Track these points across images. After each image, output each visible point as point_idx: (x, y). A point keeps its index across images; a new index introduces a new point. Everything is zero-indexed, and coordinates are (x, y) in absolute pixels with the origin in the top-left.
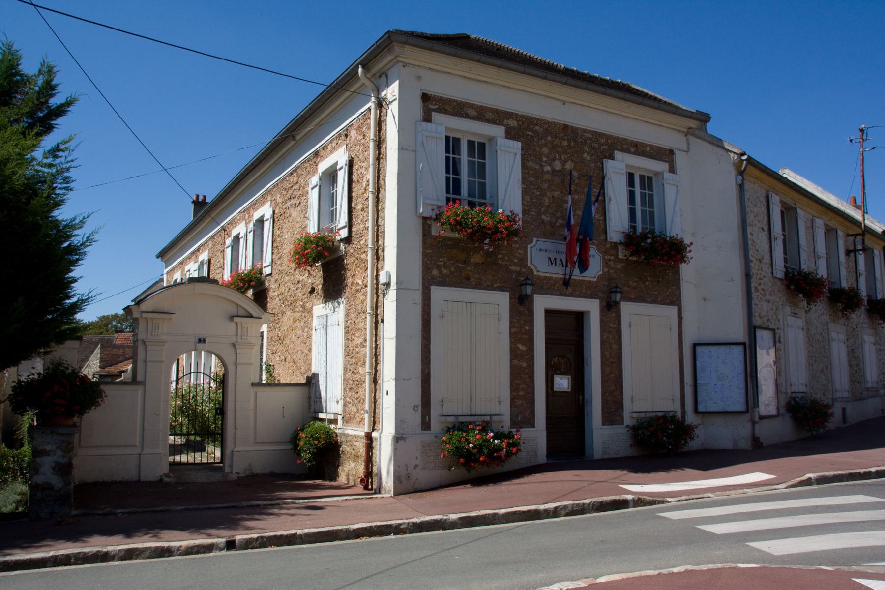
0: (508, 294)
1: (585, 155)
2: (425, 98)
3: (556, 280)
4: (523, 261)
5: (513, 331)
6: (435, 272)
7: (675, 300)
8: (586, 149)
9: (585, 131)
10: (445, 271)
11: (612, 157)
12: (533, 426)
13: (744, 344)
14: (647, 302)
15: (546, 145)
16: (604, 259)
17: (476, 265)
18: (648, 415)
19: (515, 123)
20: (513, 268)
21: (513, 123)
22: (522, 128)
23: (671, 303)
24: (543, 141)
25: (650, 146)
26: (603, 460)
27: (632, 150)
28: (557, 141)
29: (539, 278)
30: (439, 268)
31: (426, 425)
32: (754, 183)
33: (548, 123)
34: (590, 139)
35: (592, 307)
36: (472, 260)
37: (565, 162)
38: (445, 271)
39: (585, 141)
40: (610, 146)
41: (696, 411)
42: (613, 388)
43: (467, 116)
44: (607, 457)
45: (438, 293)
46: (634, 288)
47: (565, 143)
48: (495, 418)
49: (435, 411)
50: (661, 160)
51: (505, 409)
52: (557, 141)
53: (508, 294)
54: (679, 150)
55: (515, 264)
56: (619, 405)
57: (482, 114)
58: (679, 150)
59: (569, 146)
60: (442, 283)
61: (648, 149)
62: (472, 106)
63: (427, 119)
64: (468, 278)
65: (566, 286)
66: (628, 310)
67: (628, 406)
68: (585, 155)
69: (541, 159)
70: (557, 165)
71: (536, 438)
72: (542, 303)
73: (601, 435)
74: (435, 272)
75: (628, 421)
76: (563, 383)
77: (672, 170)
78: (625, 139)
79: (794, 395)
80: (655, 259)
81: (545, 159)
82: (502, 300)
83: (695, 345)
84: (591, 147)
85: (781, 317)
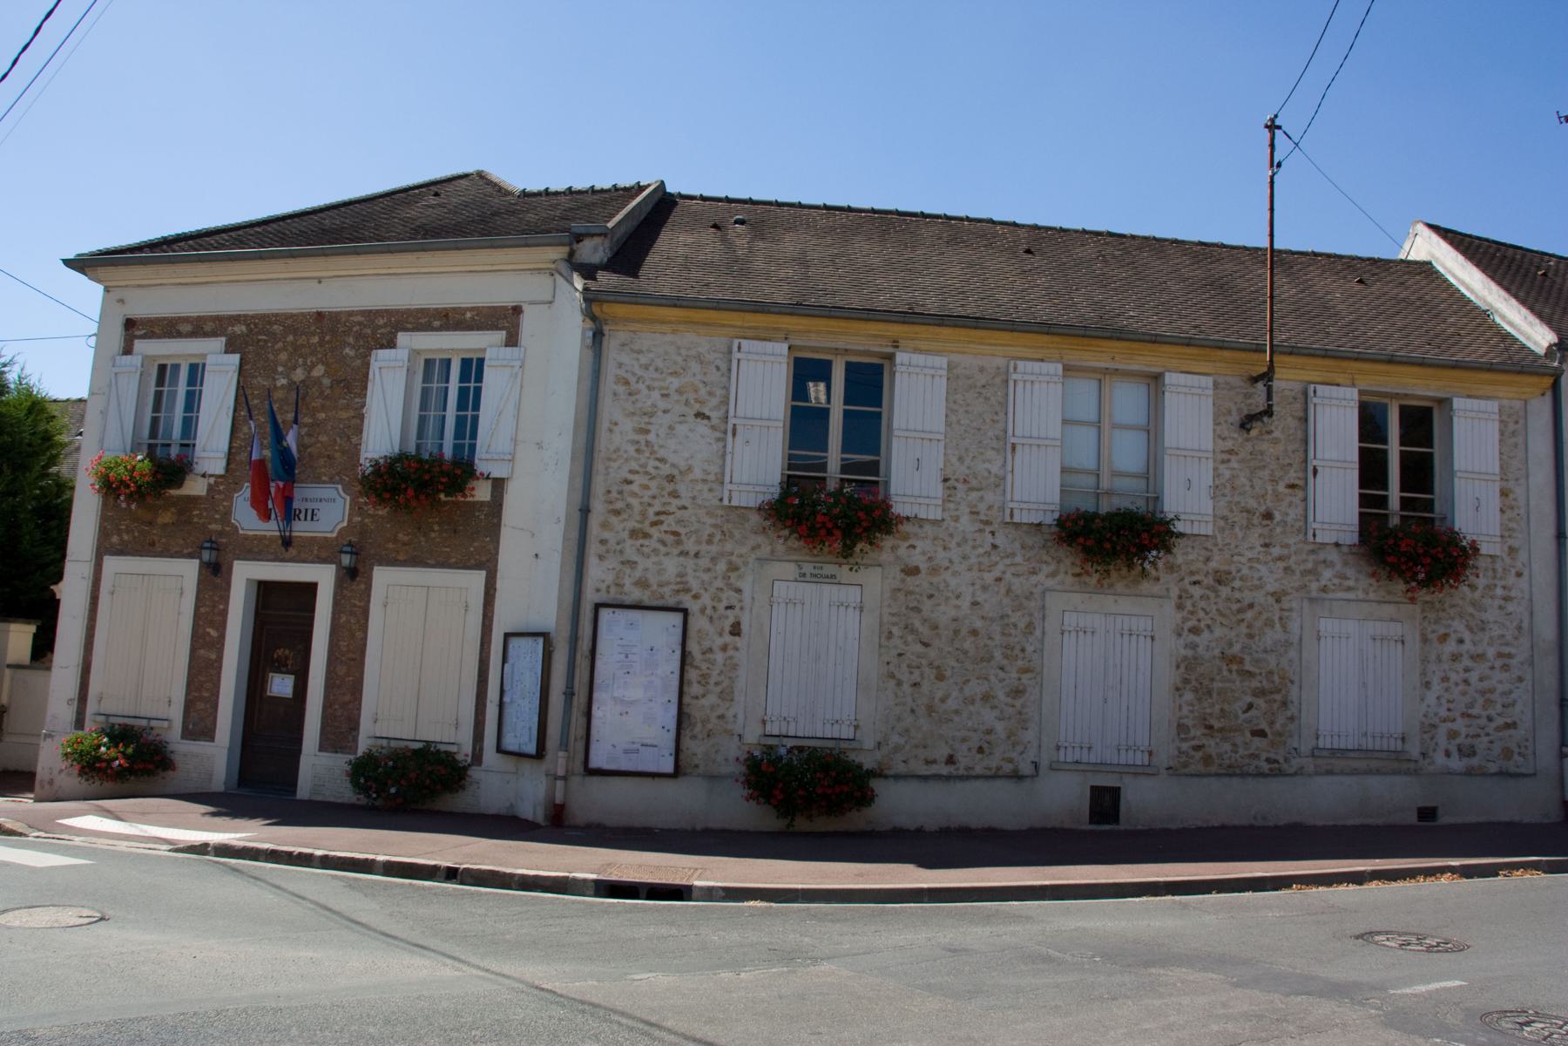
0: (236, 563)
1: (347, 350)
2: (130, 324)
3: (271, 539)
4: (227, 513)
5: (202, 610)
6: (115, 539)
7: (488, 563)
8: (351, 340)
9: (351, 314)
10: (126, 537)
11: (391, 344)
12: (212, 739)
13: (545, 635)
14: (426, 565)
15: (284, 349)
16: (354, 502)
17: (165, 525)
18: (393, 744)
19: (244, 328)
20: (213, 527)
21: (240, 329)
22: (250, 337)
23: (478, 567)
24: (280, 345)
25: (472, 309)
26: (310, 803)
27: (437, 323)
28: (302, 340)
29: (246, 538)
30: (119, 533)
31: (79, 723)
32: (674, 332)
33: (292, 316)
34: (360, 323)
35: (324, 577)
36: (160, 520)
37: (313, 366)
38: (126, 537)
39: (350, 329)
40: (383, 328)
41: (500, 750)
42: (347, 698)
43: (180, 335)
44: (319, 798)
45: (111, 564)
46: (405, 544)
47: (315, 340)
48: (153, 723)
49: (91, 707)
50: (496, 328)
51: (176, 713)
52: (302, 340)
53: (236, 563)
54: (532, 303)
55: (216, 521)
56: (354, 725)
57: (199, 327)
58: (532, 303)
59: (321, 343)
60: (121, 551)
61: (468, 315)
62: (186, 320)
63: (128, 350)
64: (153, 544)
65: (287, 547)
66: (384, 578)
67: (367, 729)
68: (347, 350)
69: (275, 371)
70: (299, 375)
71: (215, 756)
72: (245, 573)
73: (318, 767)
74: (115, 539)
75: (363, 745)
76: (281, 685)
77: (512, 341)
78: (422, 310)
79: (771, 741)
80: (433, 498)
81: (280, 369)
82: (188, 570)
83: (507, 636)
84: (359, 336)
85: (746, 585)
